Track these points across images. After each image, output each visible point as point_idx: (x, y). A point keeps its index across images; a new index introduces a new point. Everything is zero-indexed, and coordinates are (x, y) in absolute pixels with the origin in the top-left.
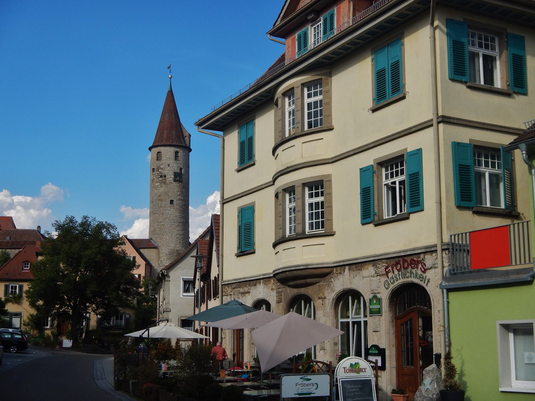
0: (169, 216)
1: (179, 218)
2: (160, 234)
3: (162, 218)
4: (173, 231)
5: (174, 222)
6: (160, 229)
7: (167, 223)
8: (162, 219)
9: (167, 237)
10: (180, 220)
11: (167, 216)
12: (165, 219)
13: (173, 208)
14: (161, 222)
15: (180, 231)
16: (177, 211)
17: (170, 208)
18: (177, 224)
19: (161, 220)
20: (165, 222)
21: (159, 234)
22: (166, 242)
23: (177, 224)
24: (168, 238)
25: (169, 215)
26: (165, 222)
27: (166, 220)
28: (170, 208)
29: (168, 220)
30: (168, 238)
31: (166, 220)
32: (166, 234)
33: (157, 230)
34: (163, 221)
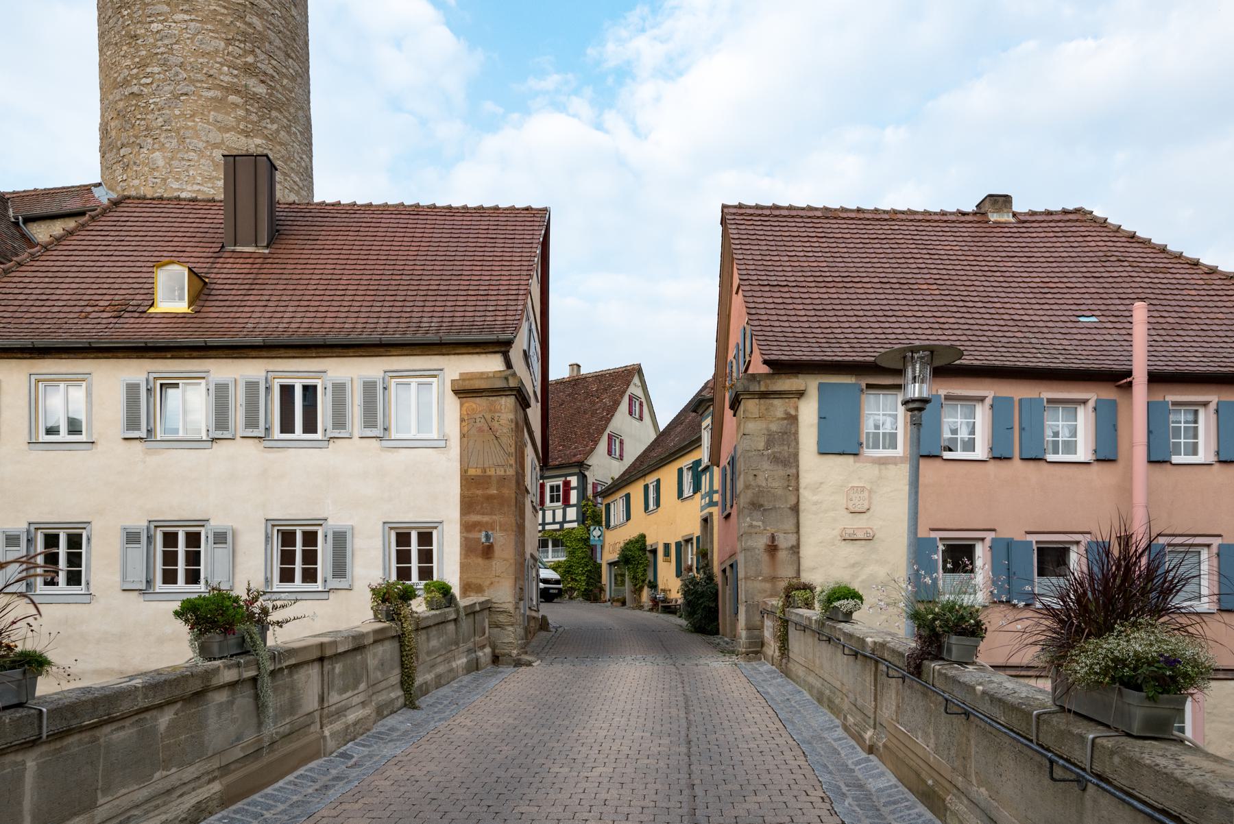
0: (162, 49)
1: (222, 64)
2: (123, 146)
3: (128, 62)
4: (187, 128)
5: (193, 82)
6: (124, 116)
7: (154, 85)
8: (128, 67)
9: (157, 153)
10: (227, 79)
11: (155, 46)
12: (142, 65)
13: (184, 7)
14: (126, 83)
15: (227, 129)
16: (209, 27)
17: (165, 8)
18: (211, 94)
19: (126, 72)
20: (144, 81)
21: (119, 143)
22: (150, 179)
23: (211, 94)
24: (161, 163)
25: (166, 42)
26: (144, 81)
27: (149, 70)
28: (168, 4)
29: (156, 70)
30: (161, 163)
31: (149, 70)
32: (150, 140)
33: (113, 124)
34: (136, 77)
